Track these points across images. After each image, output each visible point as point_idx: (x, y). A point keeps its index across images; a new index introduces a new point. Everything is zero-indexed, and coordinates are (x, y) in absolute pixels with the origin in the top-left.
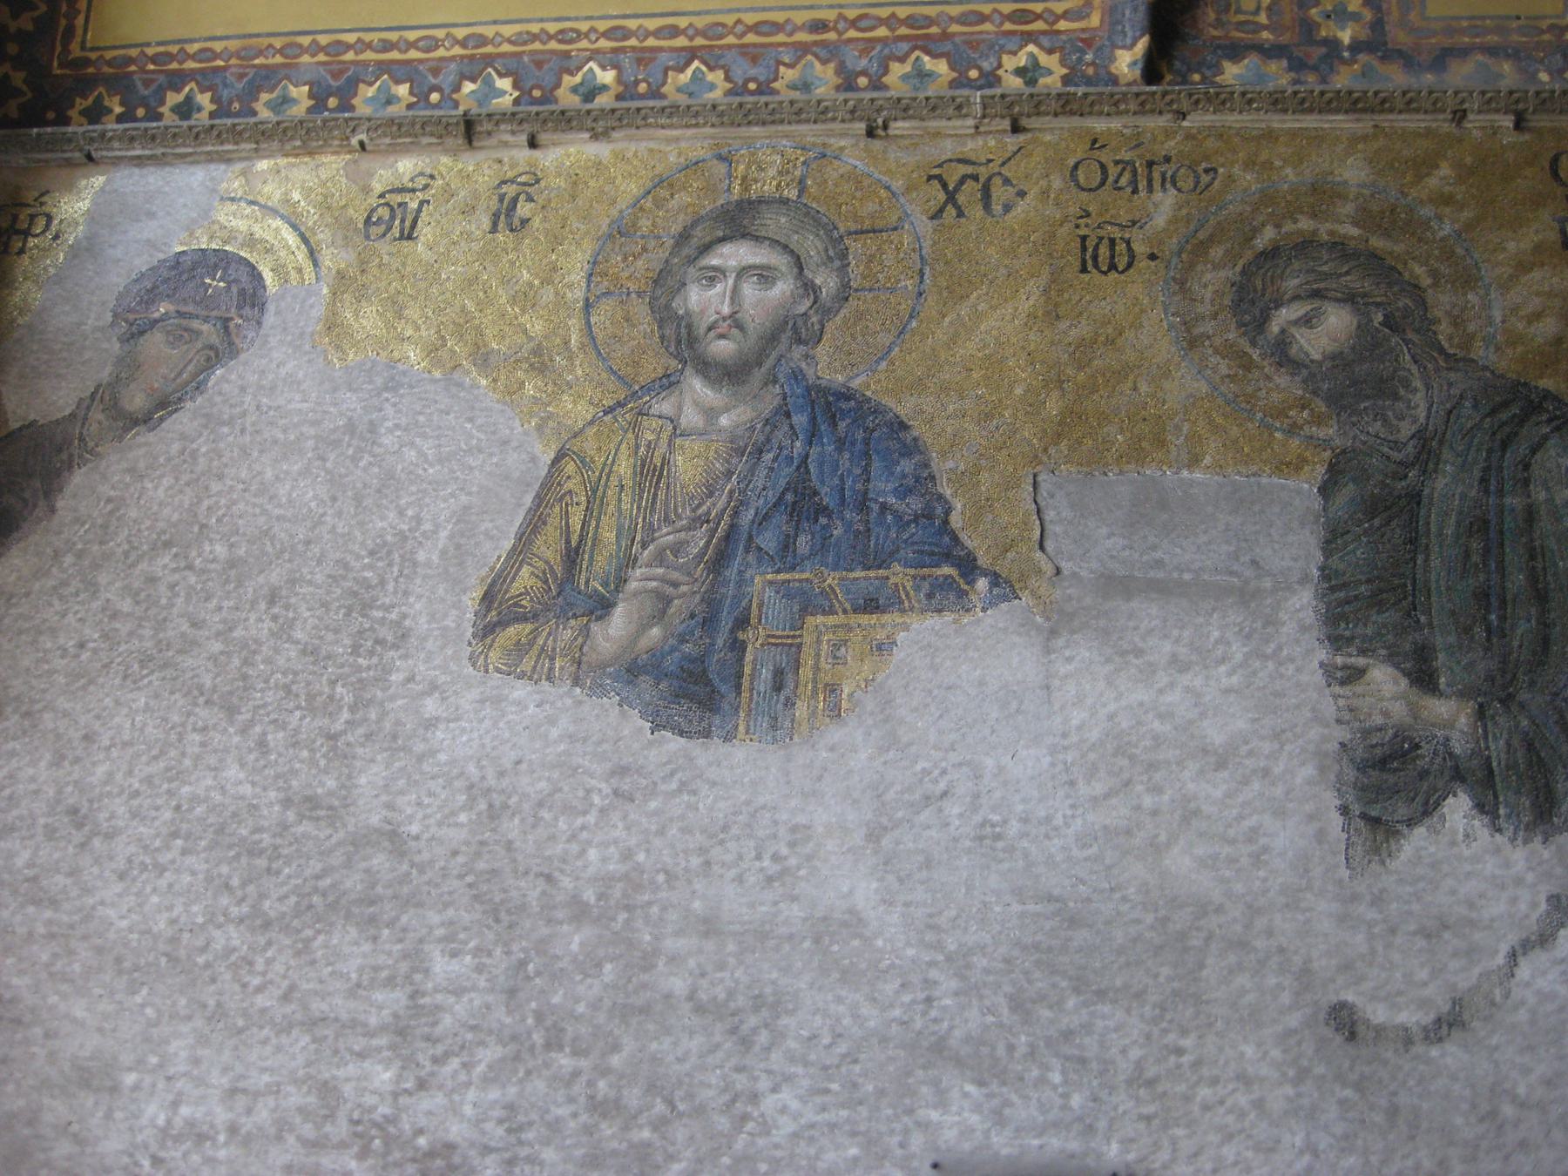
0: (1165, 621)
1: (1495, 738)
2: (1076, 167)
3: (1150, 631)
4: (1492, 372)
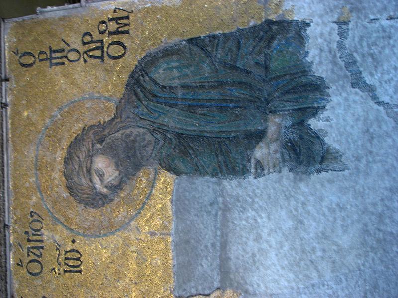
0: (239, 243)
1: (285, 106)
2: (31, 274)
3: (244, 250)
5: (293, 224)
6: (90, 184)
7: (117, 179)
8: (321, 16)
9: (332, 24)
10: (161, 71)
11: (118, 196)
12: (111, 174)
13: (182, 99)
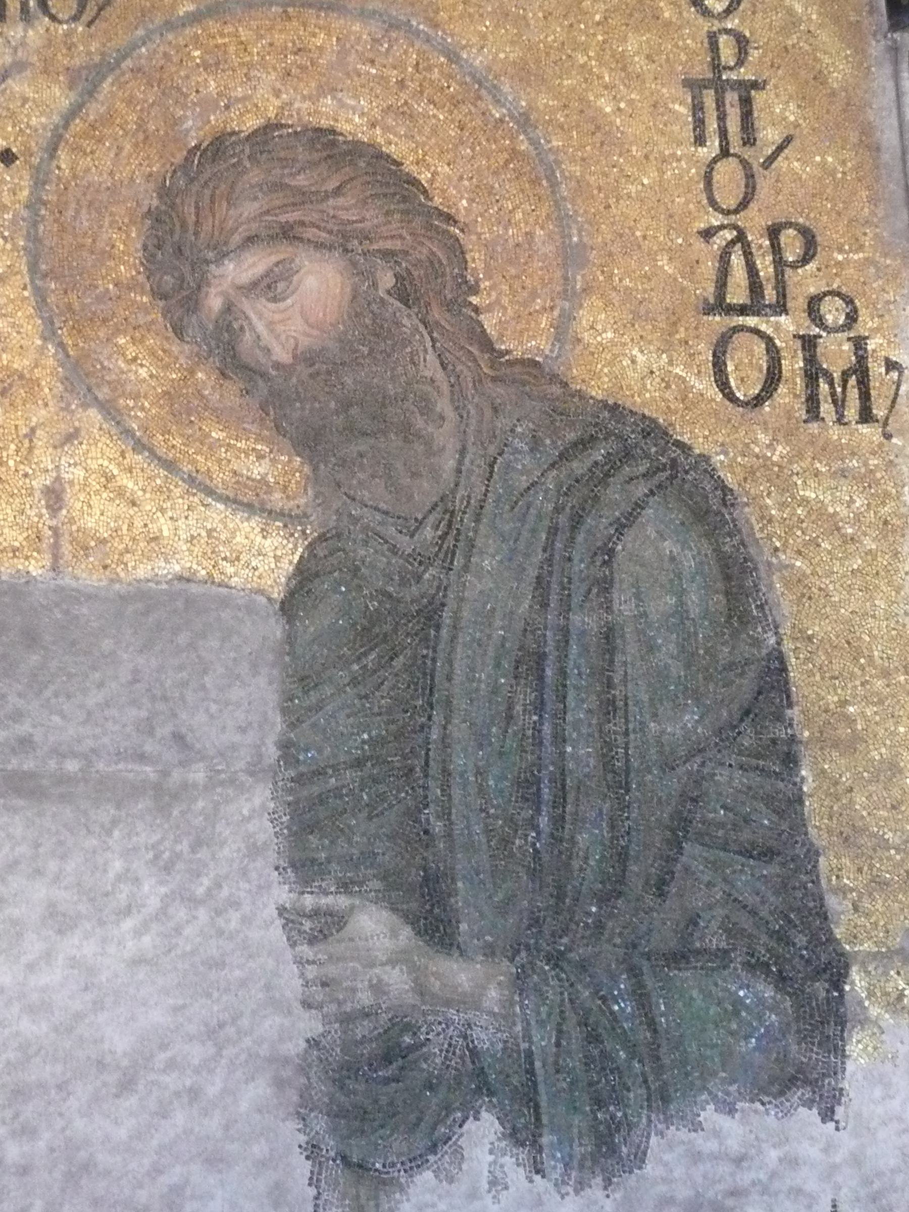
0: (37, 846)
4: (565, 385)
5: (119, 1051)
6: (237, 239)
8: (856, 1160)
9: (830, 1197)
10: (668, 546)
11: (199, 359)
12: (280, 328)
13: (565, 632)
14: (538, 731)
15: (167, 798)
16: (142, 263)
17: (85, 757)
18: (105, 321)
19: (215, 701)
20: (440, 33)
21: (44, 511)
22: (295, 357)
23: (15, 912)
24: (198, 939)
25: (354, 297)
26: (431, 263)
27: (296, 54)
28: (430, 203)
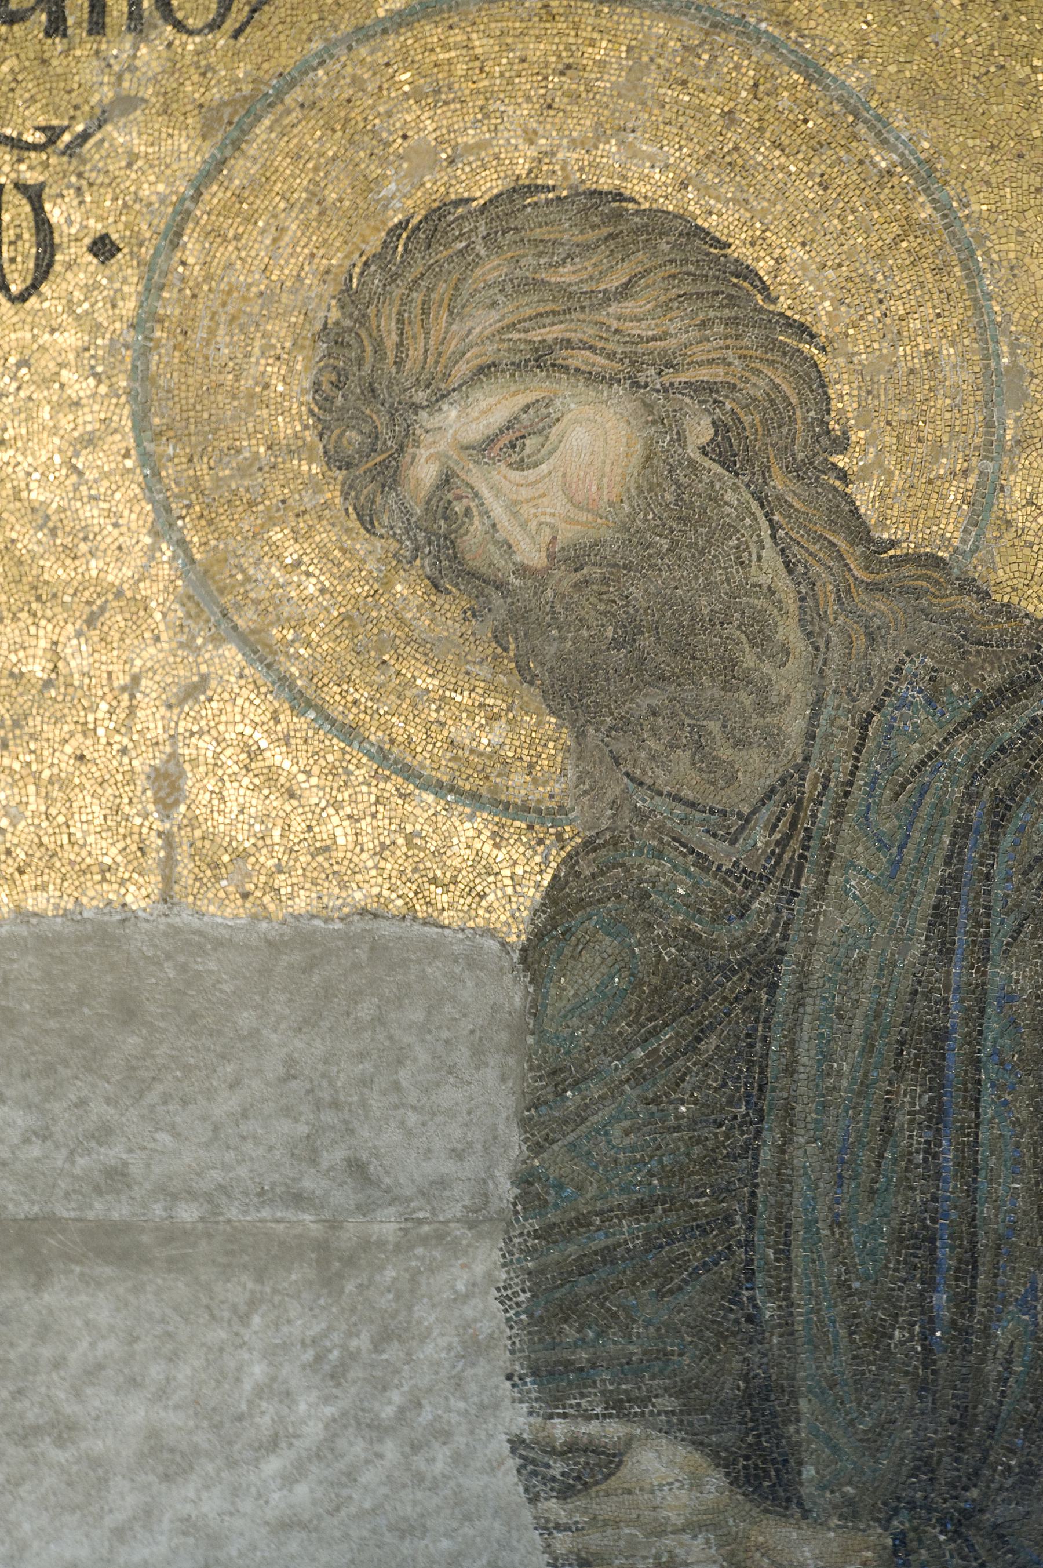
3: (94, 1371)
6: (463, 369)
7: (496, 555)
12: (527, 510)
14: (931, 1154)
15: (337, 1264)
16: (311, 412)
17: (209, 1198)
18: (252, 504)
19: (414, 1108)
20: (793, 35)
21: (151, 807)
22: (551, 556)
23: (98, 1446)
24: (385, 1490)
25: (648, 458)
26: (772, 402)
27: (562, 73)
28: (771, 308)
